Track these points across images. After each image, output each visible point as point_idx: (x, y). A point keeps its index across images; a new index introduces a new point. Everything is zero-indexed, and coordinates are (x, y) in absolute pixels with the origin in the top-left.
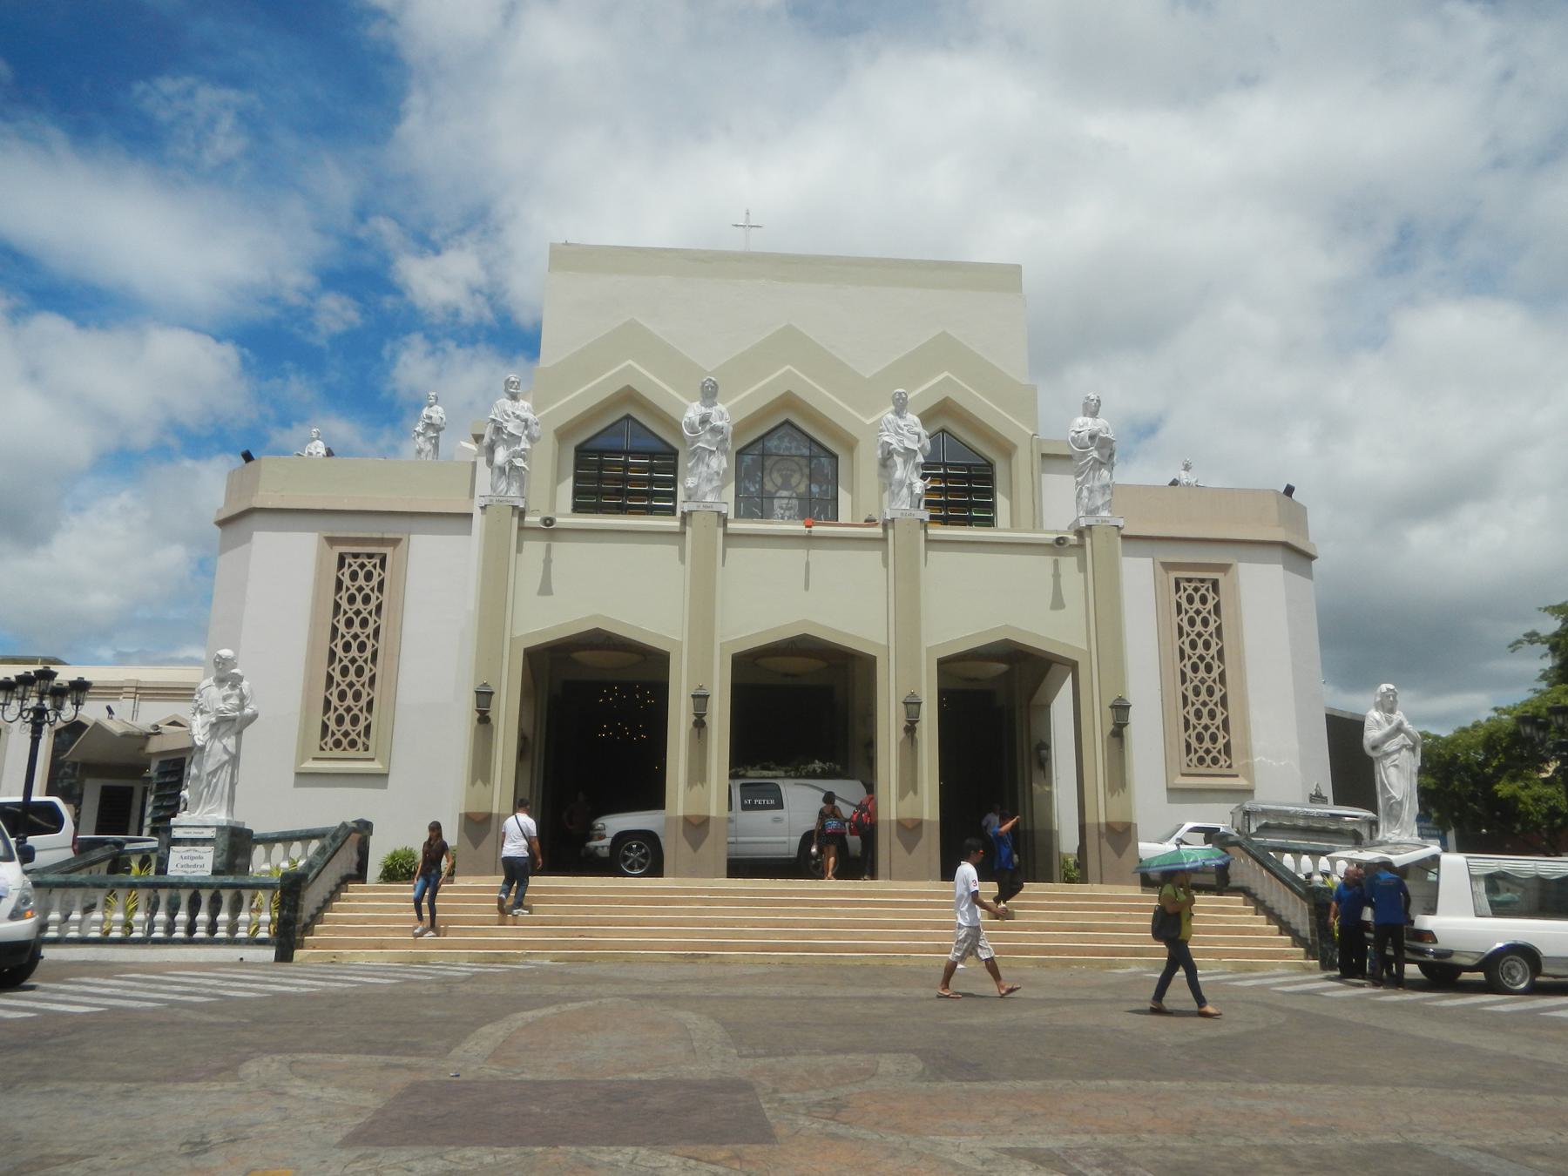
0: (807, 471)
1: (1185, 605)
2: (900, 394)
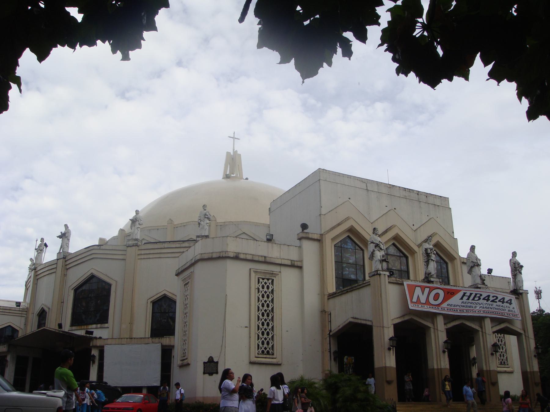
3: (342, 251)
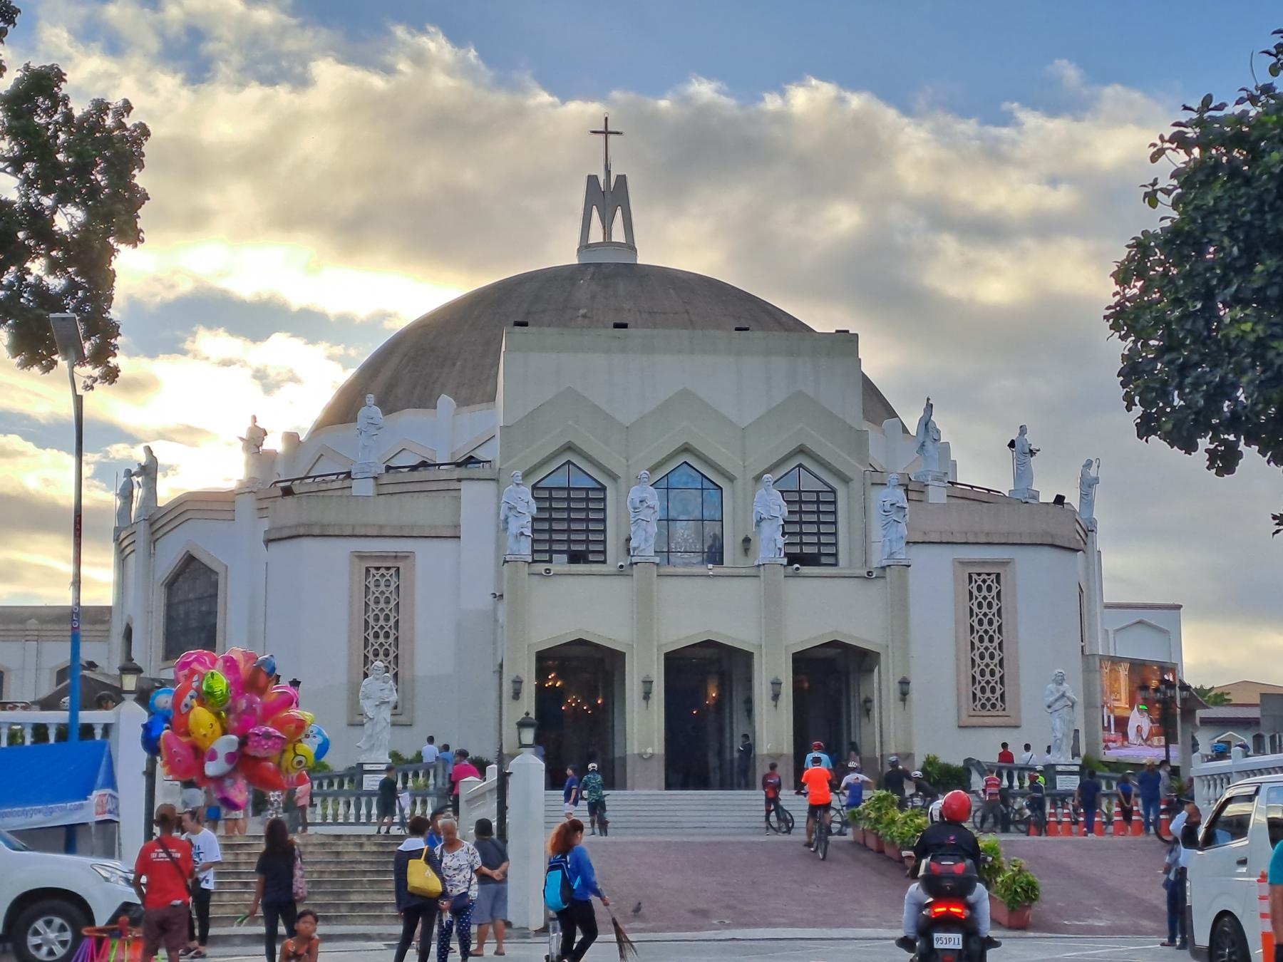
1: (975, 593)
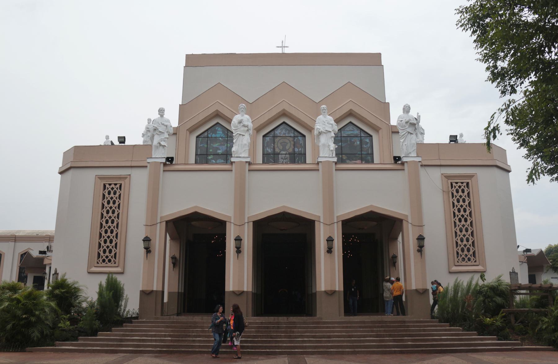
0: (292, 143)
2: (324, 107)
3: (209, 141)
